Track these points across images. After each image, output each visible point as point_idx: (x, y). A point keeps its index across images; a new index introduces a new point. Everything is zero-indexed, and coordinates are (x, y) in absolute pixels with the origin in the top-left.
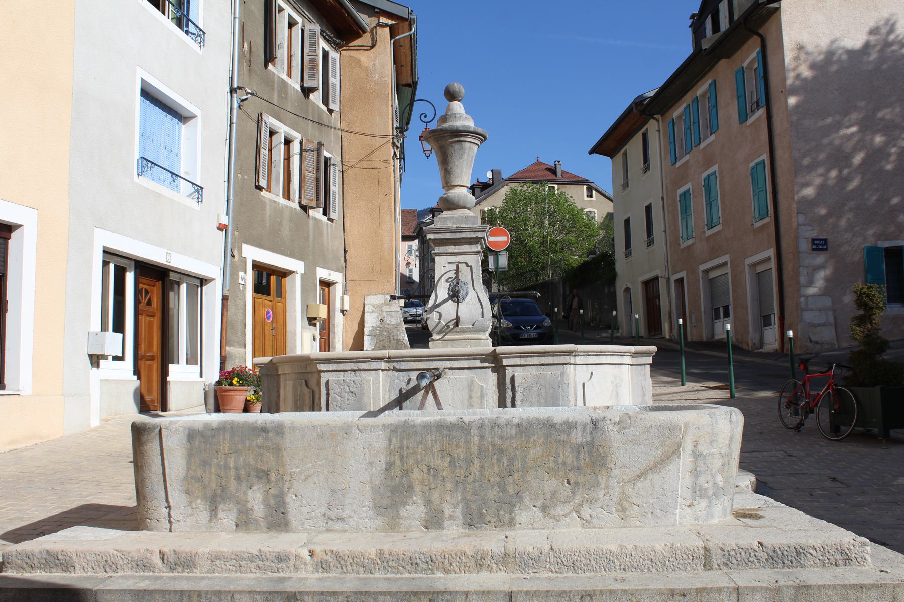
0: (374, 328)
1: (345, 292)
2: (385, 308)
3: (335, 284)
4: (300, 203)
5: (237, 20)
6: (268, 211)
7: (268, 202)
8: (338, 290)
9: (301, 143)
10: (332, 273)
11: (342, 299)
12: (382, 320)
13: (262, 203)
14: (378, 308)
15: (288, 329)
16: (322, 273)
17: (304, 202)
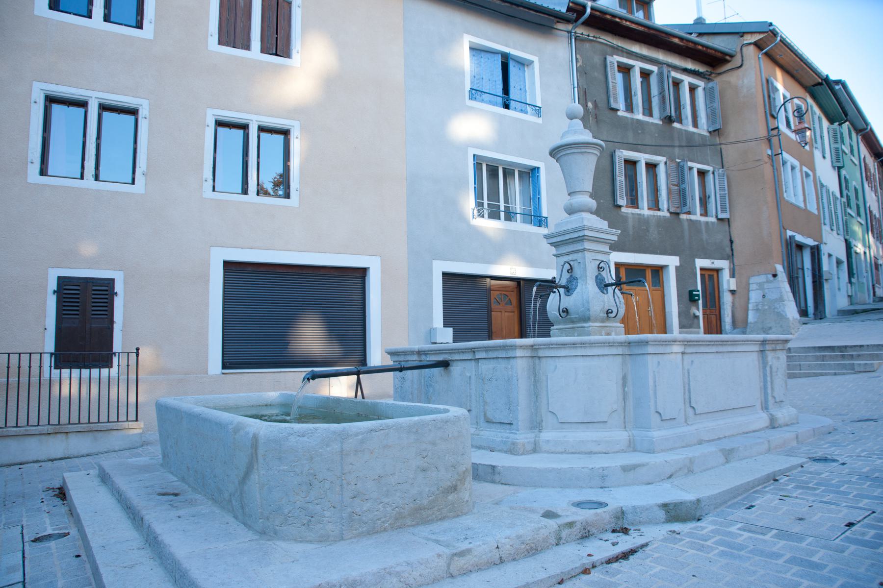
0: (757, 304)
1: (733, 275)
2: (766, 286)
3: (722, 269)
4: (668, 210)
5: (576, 89)
6: (631, 223)
7: (630, 216)
8: (726, 275)
9: (666, 163)
10: (716, 261)
11: (729, 281)
12: (764, 296)
13: (625, 218)
14: (760, 286)
15: (667, 310)
16: (701, 263)
17: (672, 210)
